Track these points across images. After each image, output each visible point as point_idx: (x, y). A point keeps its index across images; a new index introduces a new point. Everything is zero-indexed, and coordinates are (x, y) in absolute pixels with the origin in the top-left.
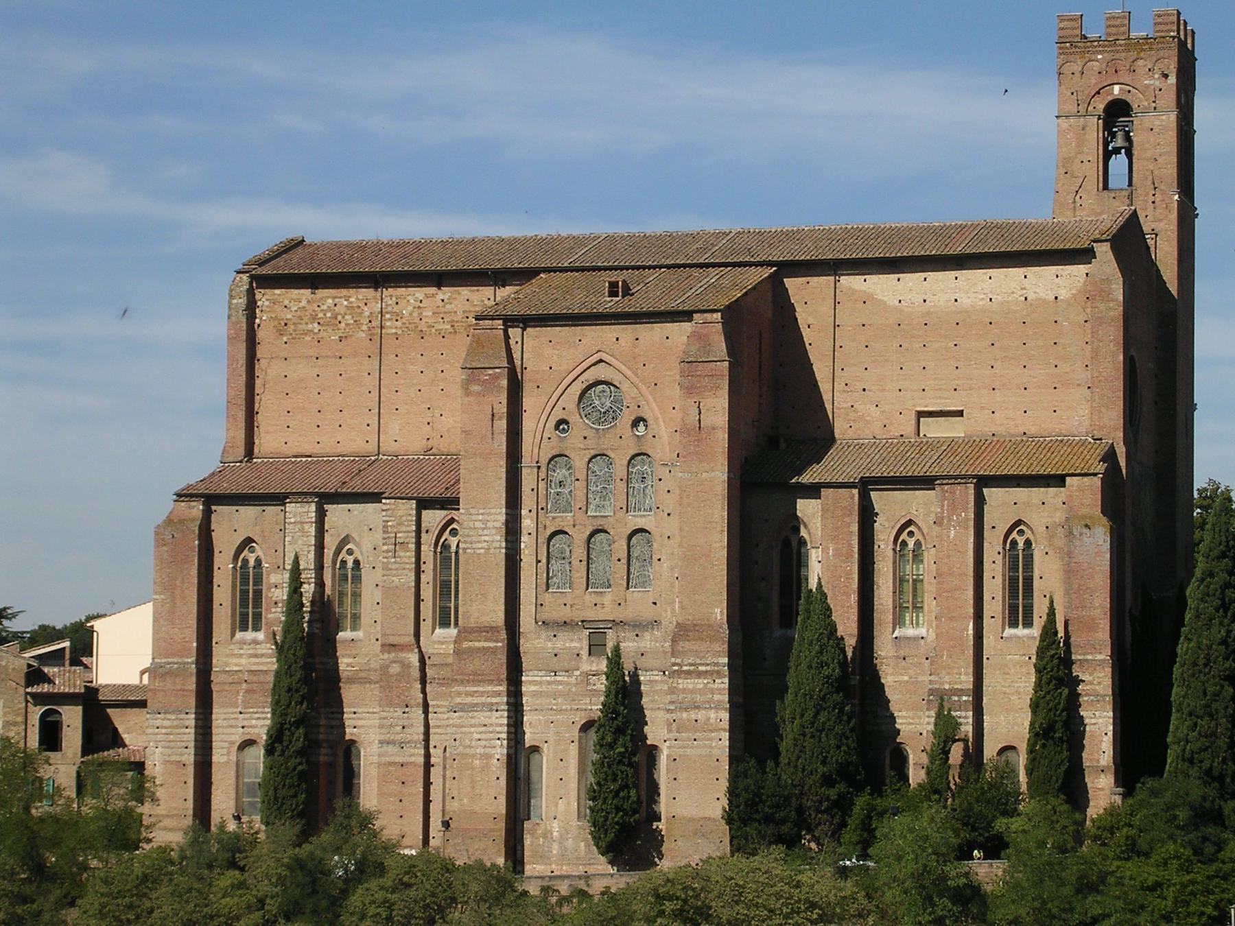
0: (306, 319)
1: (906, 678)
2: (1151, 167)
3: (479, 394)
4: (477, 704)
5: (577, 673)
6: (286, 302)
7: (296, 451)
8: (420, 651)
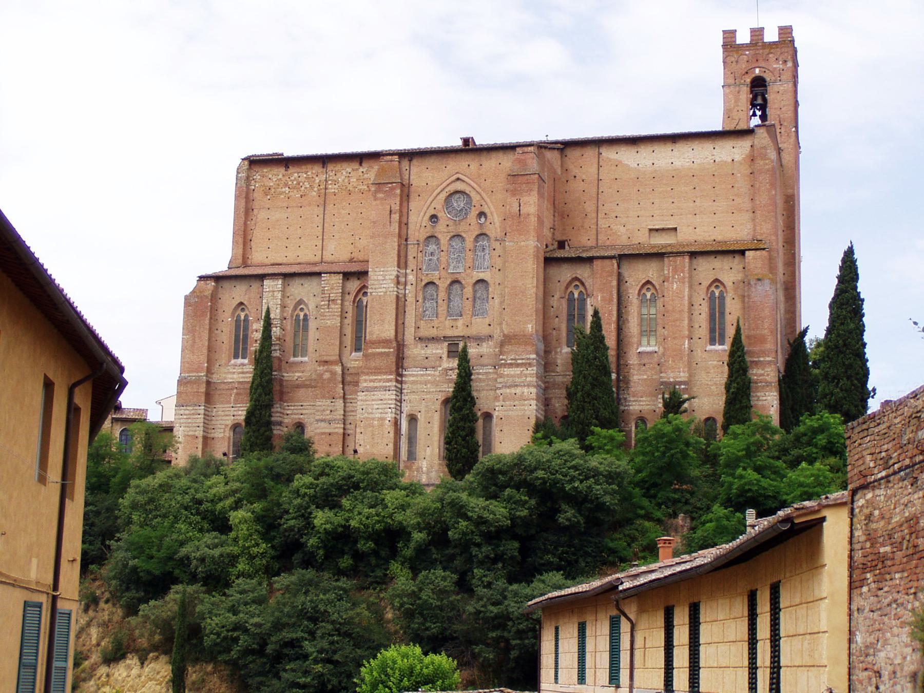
0: (281, 185)
1: (645, 377)
2: (778, 113)
3: (382, 199)
4: (376, 387)
5: (440, 369)
6: (270, 176)
7: (272, 262)
8: (342, 365)
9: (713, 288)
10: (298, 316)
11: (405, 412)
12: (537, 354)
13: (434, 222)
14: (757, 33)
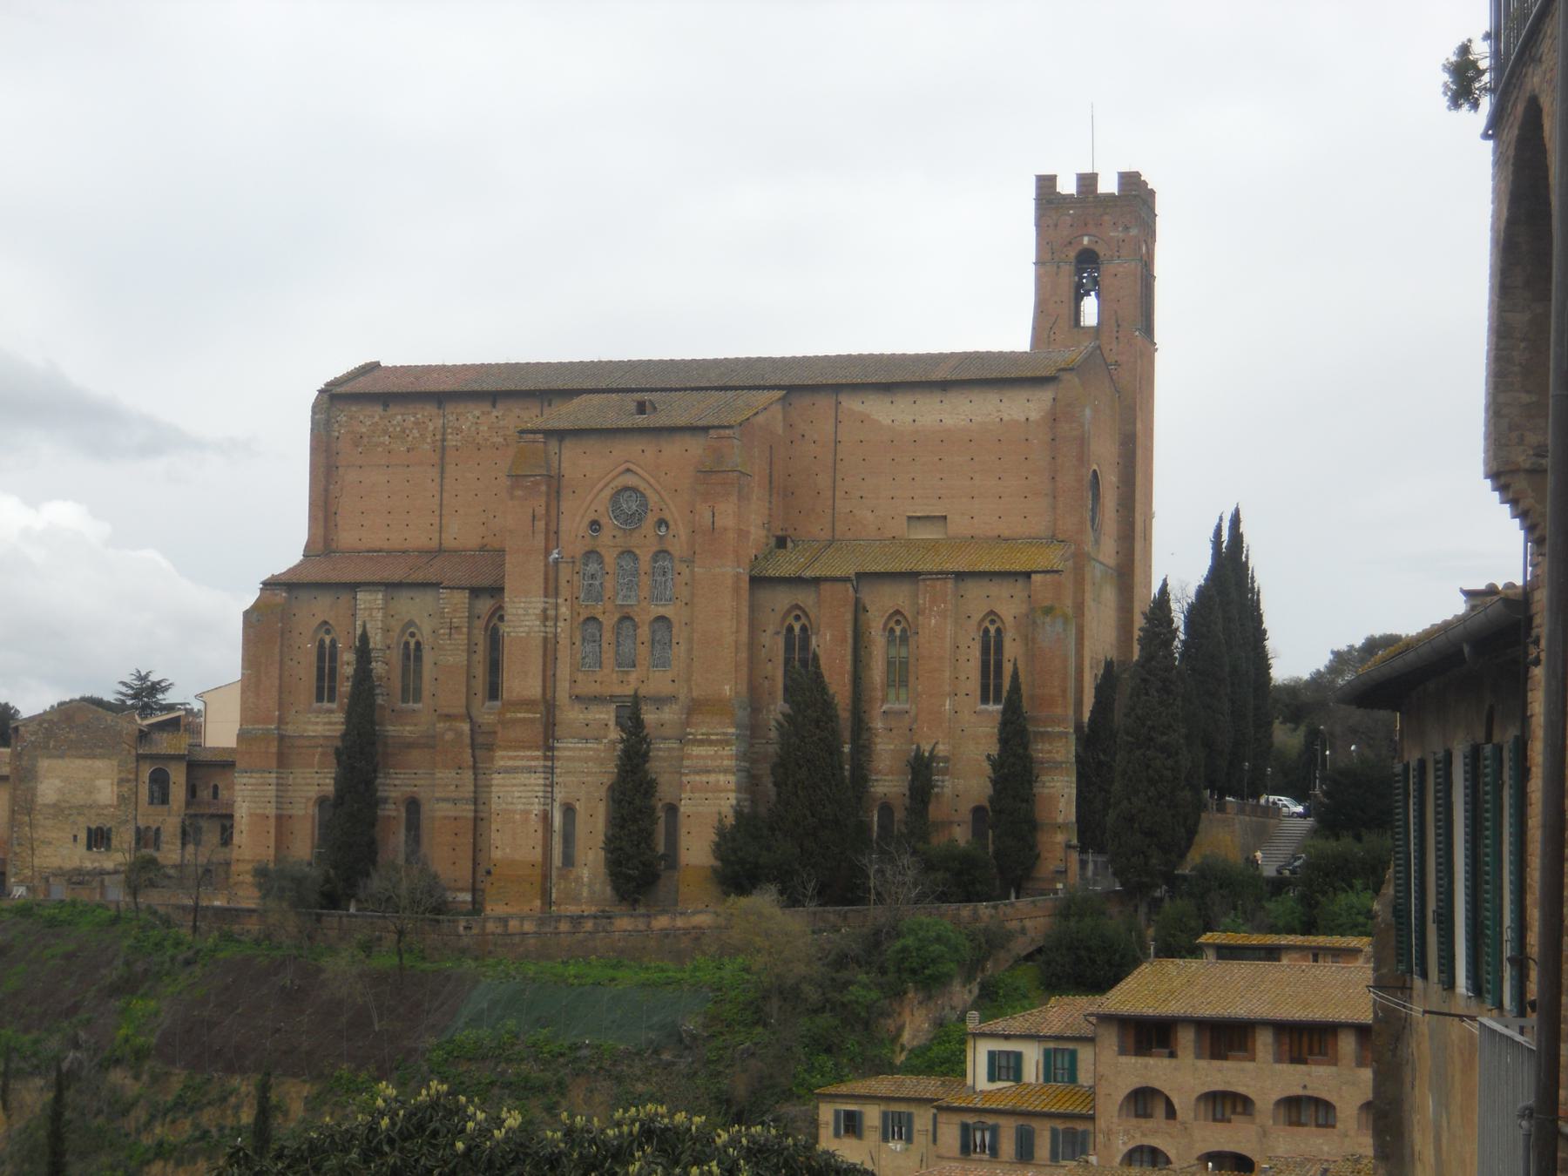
1: (892, 747)
5: (605, 741)
6: (361, 418)
8: (471, 720)
10: (407, 644)
11: (558, 800)
12: (738, 726)
14: (1087, 182)
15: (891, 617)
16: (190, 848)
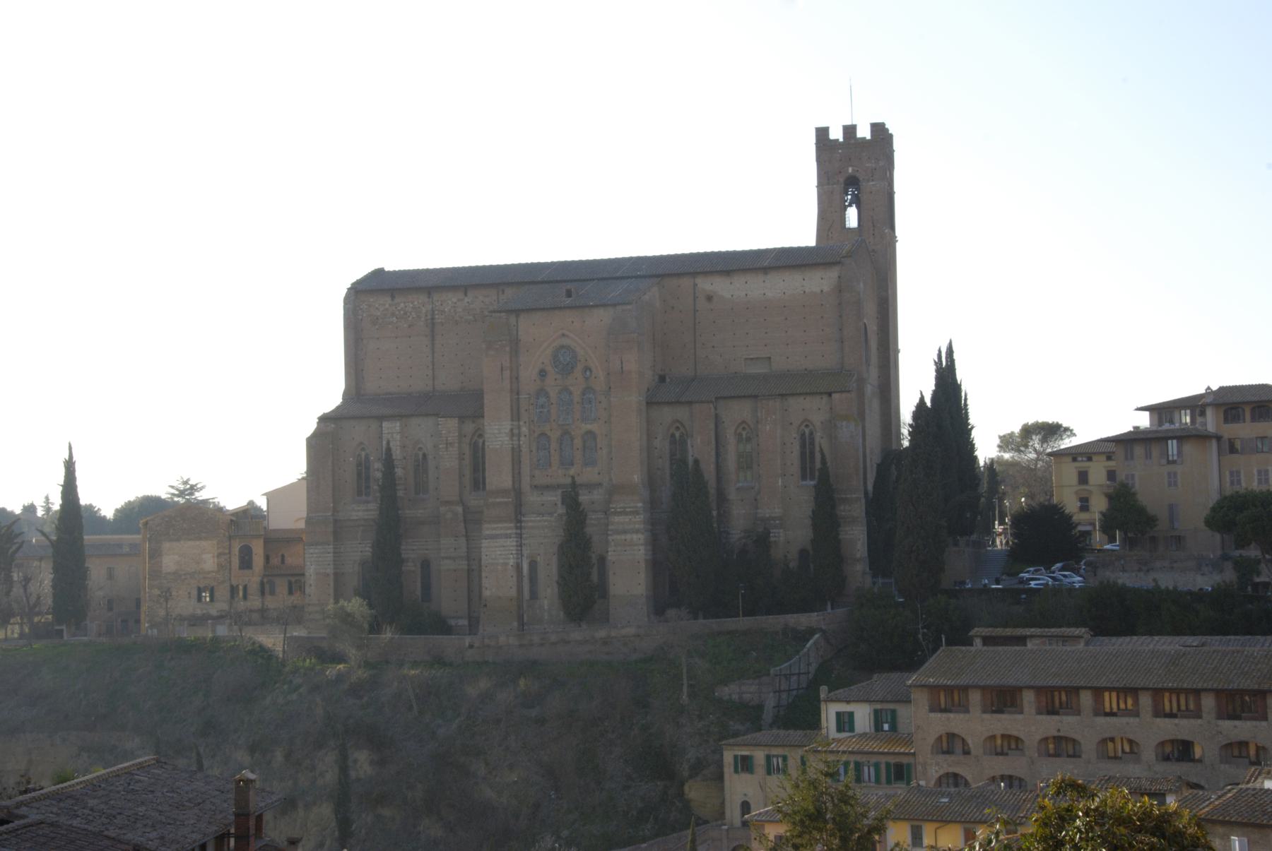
6: (377, 306)
9: (803, 427)
11: (525, 555)
13: (543, 376)
14: (850, 130)
15: (738, 427)
16: (269, 598)
